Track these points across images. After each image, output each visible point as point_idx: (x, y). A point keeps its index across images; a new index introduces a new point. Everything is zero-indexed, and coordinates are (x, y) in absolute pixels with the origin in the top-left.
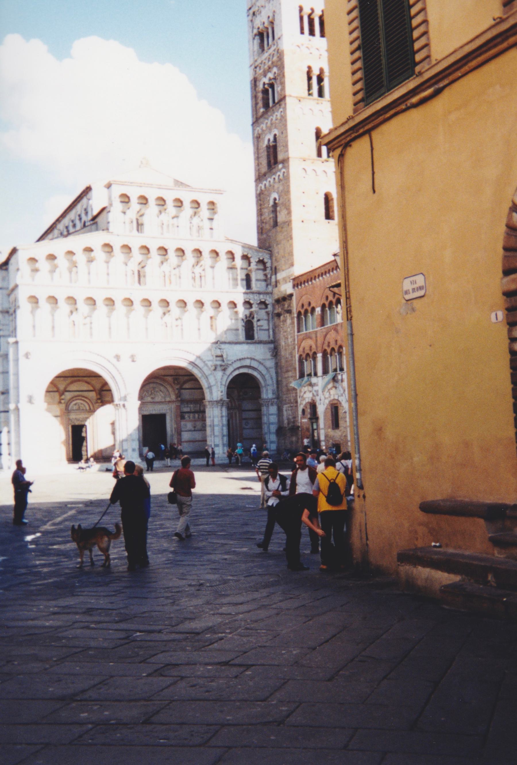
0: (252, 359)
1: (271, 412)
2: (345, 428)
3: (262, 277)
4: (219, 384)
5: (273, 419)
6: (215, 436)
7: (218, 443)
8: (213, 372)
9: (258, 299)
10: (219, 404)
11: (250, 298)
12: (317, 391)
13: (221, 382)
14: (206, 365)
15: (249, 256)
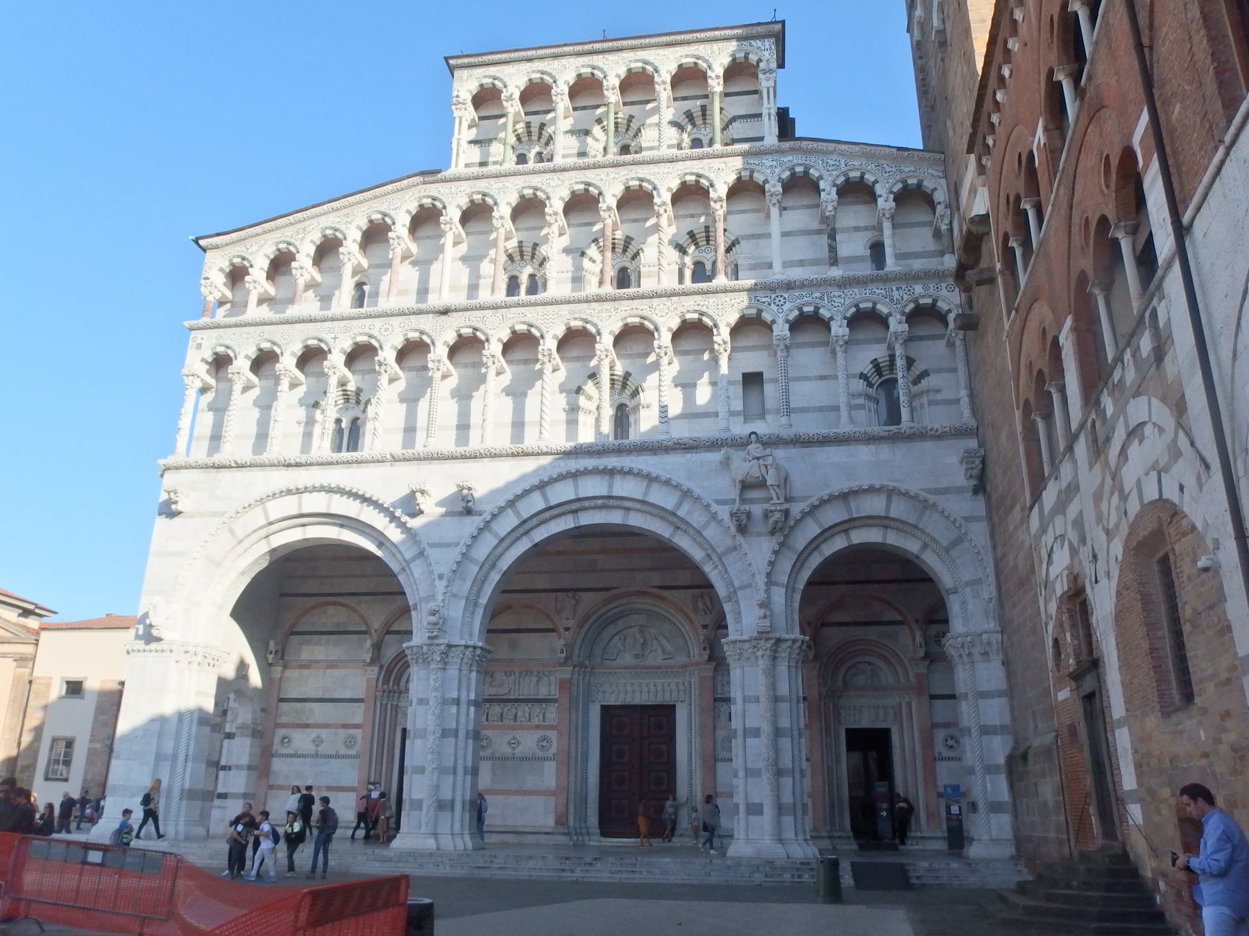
0: (891, 493)
1: (985, 687)
2: (1228, 681)
3: (931, 245)
4: (761, 580)
5: (996, 711)
6: (749, 773)
7: (757, 801)
8: (739, 538)
9: (905, 297)
10: (760, 653)
11: (874, 297)
12: (1079, 523)
13: (769, 575)
14: (714, 517)
15: (869, 178)
